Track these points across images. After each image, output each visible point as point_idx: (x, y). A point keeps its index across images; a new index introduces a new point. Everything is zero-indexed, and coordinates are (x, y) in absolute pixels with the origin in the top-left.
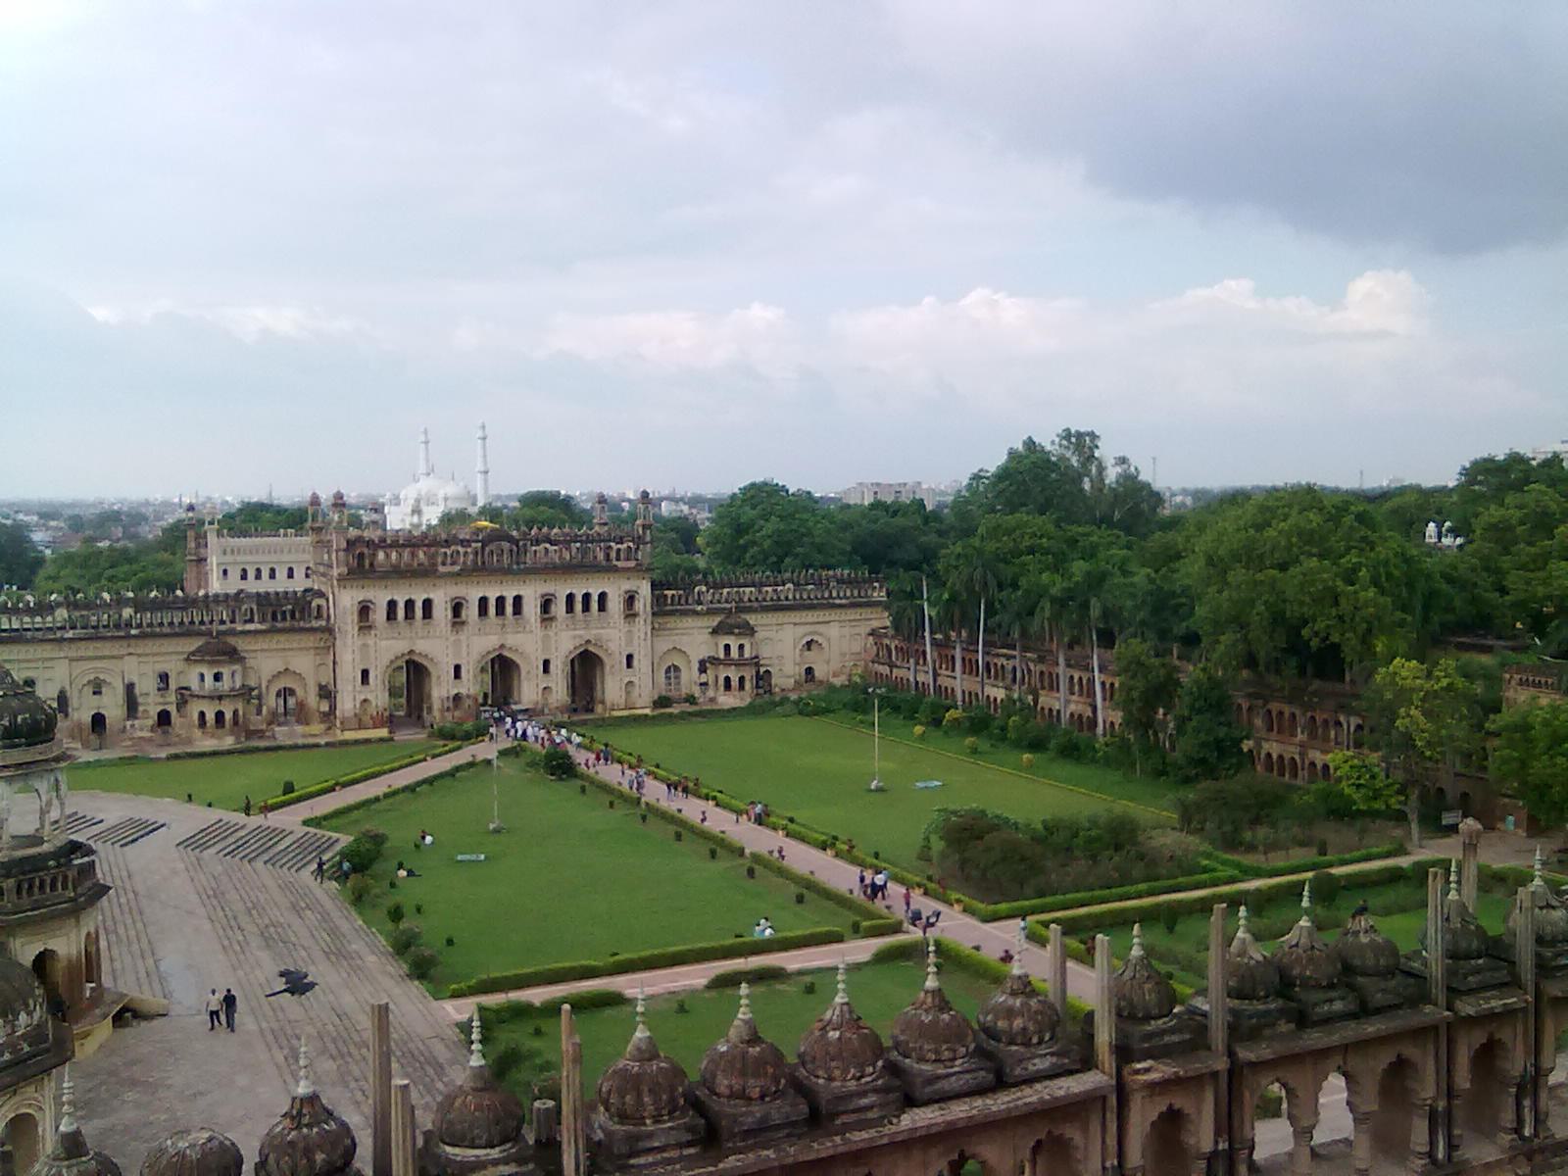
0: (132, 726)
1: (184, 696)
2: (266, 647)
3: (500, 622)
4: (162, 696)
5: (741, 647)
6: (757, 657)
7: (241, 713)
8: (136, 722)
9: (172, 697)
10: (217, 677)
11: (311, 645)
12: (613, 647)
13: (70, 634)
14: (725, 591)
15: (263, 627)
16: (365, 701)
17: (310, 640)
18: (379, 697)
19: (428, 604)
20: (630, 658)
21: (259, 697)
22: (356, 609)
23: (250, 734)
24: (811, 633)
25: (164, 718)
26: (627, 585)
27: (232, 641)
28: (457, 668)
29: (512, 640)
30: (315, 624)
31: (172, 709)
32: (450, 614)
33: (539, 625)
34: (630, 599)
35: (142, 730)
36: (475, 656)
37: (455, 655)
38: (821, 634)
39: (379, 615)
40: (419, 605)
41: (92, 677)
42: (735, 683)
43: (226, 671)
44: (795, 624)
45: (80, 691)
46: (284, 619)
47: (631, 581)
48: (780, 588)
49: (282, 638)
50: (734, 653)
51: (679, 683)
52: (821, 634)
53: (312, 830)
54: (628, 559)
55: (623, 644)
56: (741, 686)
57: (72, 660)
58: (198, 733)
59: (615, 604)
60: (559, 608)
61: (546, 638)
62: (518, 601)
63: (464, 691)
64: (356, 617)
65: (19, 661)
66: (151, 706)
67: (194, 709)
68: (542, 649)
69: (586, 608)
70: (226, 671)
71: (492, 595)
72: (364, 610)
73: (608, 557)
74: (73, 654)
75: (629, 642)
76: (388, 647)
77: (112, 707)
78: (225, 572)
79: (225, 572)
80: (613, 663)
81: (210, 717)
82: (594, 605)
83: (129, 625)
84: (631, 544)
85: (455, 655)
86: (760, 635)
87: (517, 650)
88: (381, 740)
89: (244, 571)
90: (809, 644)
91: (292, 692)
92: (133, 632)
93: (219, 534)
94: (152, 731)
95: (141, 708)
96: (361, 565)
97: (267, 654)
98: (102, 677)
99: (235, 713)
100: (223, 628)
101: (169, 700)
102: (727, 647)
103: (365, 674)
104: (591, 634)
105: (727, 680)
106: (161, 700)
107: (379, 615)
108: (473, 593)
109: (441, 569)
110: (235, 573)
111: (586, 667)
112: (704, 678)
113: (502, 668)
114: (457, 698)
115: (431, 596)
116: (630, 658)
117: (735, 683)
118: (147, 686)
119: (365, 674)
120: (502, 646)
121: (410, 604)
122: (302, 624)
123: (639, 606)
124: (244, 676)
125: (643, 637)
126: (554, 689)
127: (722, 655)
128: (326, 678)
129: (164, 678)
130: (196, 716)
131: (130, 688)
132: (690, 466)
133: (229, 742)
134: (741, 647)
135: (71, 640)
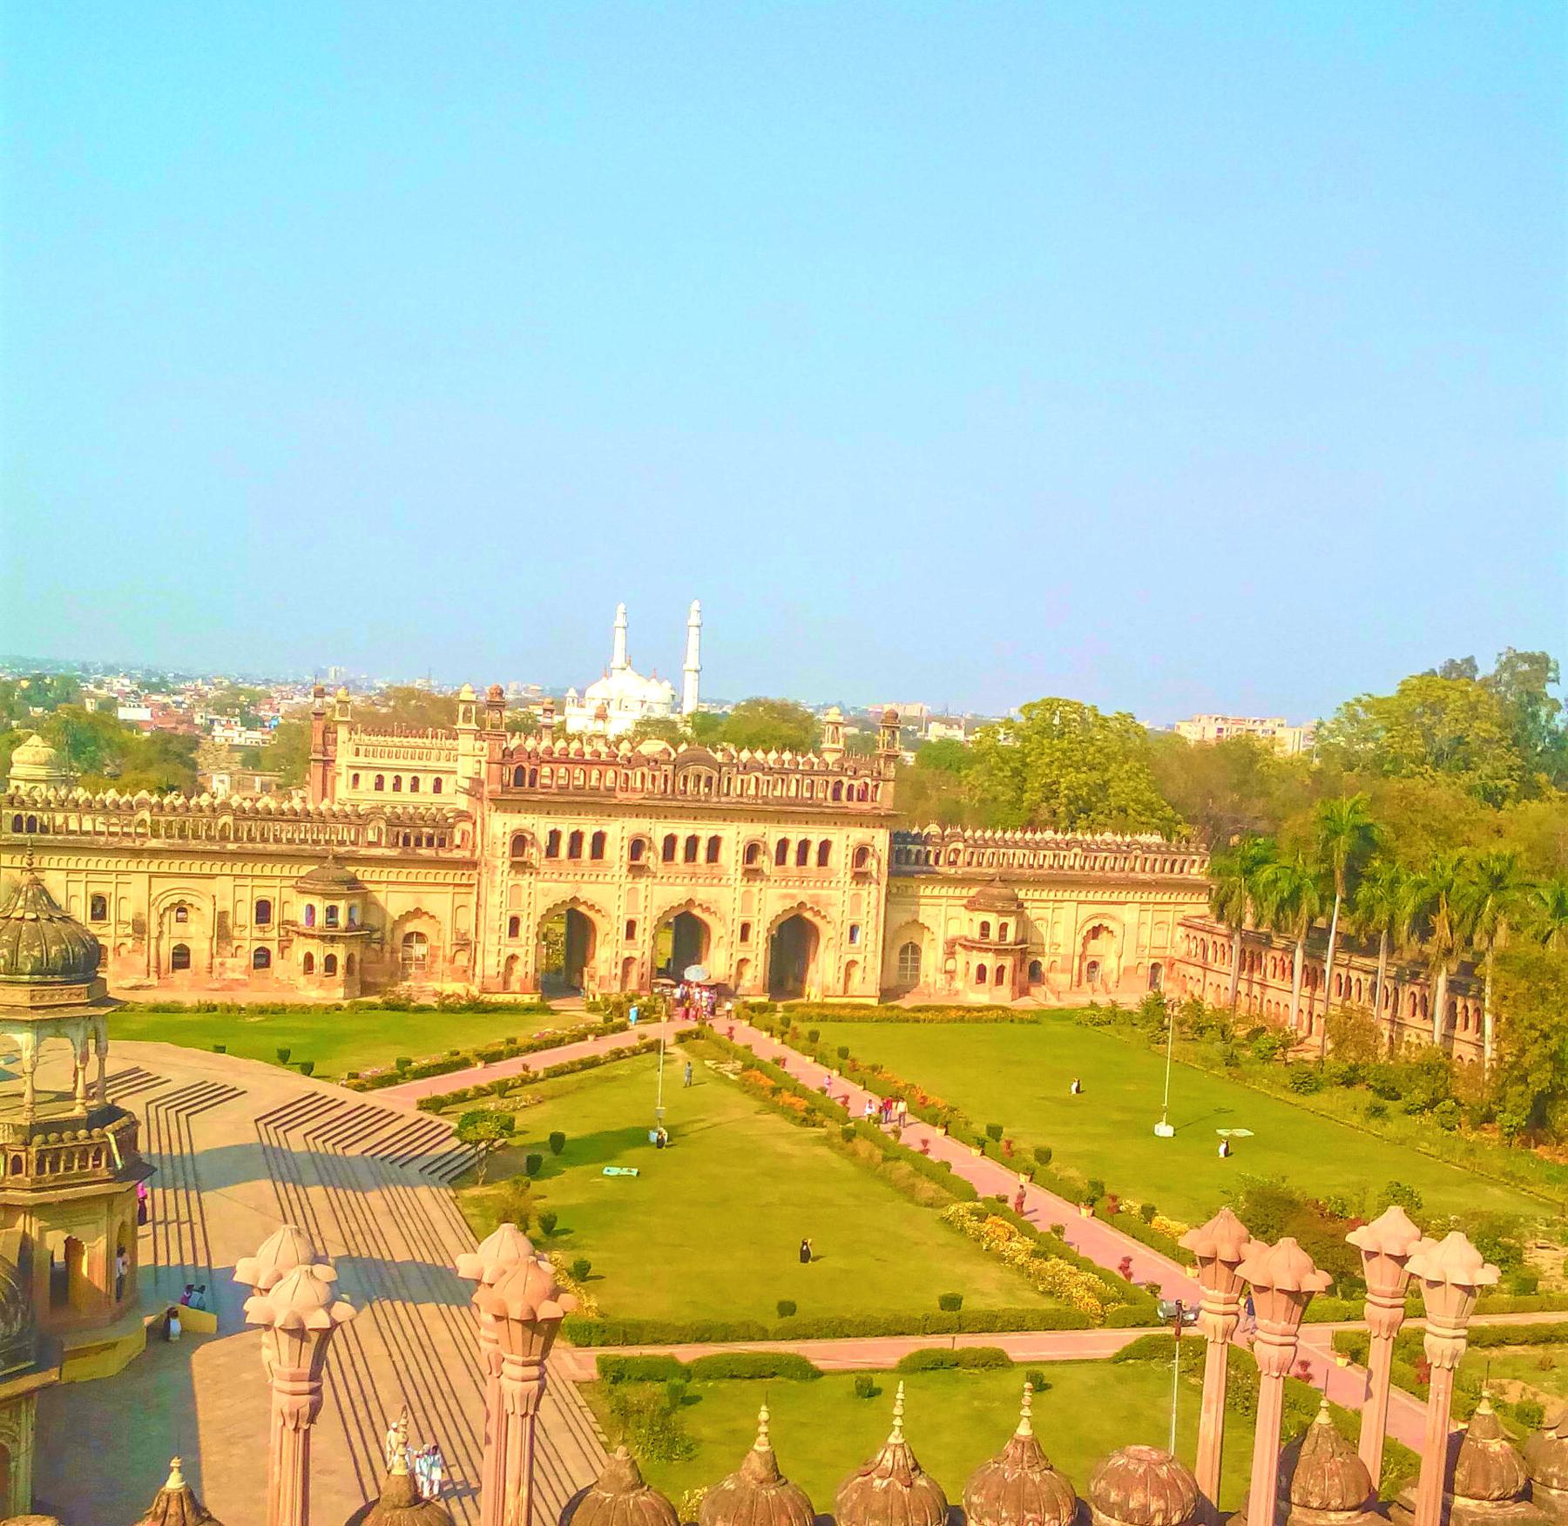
0: (222, 964)
2: (393, 878)
3: (690, 870)
4: (262, 930)
5: (1004, 927)
6: (1023, 941)
7: (357, 958)
8: (230, 962)
9: (275, 934)
10: (332, 911)
11: (449, 880)
12: (834, 913)
13: (153, 843)
14: (989, 851)
15: (394, 853)
16: (513, 958)
17: (450, 876)
18: (527, 949)
19: (599, 839)
20: (853, 930)
21: (381, 941)
22: (508, 839)
23: (367, 988)
24: (1103, 916)
25: (262, 959)
26: (859, 835)
29: (702, 894)
30: (457, 854)
31: (273, 947)
32: (626, 853)
33: (739, 876)
35: (233, 971)
37: (627, 908)
38: (1112, 918)
41: (176, 899)
42: (990, 975)
44: (1080, 902)
45: (161, 916)
46: (418, 843)
47: (864, 830)
48: (1062, 853)
50: (994, 934)
51: (917, 969)
52: (1112, 918)
53: (428, 1116)
54: (862, 799)
55: (847, 908)
56: (999, 981)
57: (152, 875)
58: (302, 980)
59: (840, 858)
63: (636, 954)
64: (507, 849)
65: (89, 872)
66: (249, 938)
67: (300, 948)
68: (742, 909)
69: (802, 859)
71: (683, 830)
72: (520, 842)
73: (836, 797)
74: (153, 868)
75: (856, 907)
76: (545, 891)
78: (356, 777)
79: (356, 777)
80: (830, 933)
81: (319, 960)
82: (813, 857)
83: (225, 838)
84: (868, 780)
85: (627, 908)
86: (1032, 912)
87: (708, 909)
88: (529, 1009)
89: (380, 778)
90: (1096, 932)
91: (421, 937)
92: (231, 847)
93: (352, 730)
94: (244, 973)
95: (236, 943)
96: (519, 782)
97: (396, 888)
98: (189, 899)
99: (350, 959)
100: (342, 850)
101: (267, 935)
102: (985, 926)
103: (515, 923)
104: (803, 895)
105: (982, 970)
106: (256, 934)
108: (658, 830)
109: (621, 796)
110: (368, 779)
111: (793, 940)
112: (950, 965)
113: (688, 932)
114: (628, 961)
115: (604, 829)
116: (853, 930)
117: (990, 975)
119: (515, 923)
120: (690, 902)
122: (443, 854)
123: (871, 864)
124: (365, 911)
125: (873, 903)
126: (754, 962)
127: (976, 934)
128: (466, 922)
129: (263, 911)
130: (301, 959)
131: (223, 915)
132: (965, 681)
133: (338, 995)
134: (1004, 927)
135: (155, 853)
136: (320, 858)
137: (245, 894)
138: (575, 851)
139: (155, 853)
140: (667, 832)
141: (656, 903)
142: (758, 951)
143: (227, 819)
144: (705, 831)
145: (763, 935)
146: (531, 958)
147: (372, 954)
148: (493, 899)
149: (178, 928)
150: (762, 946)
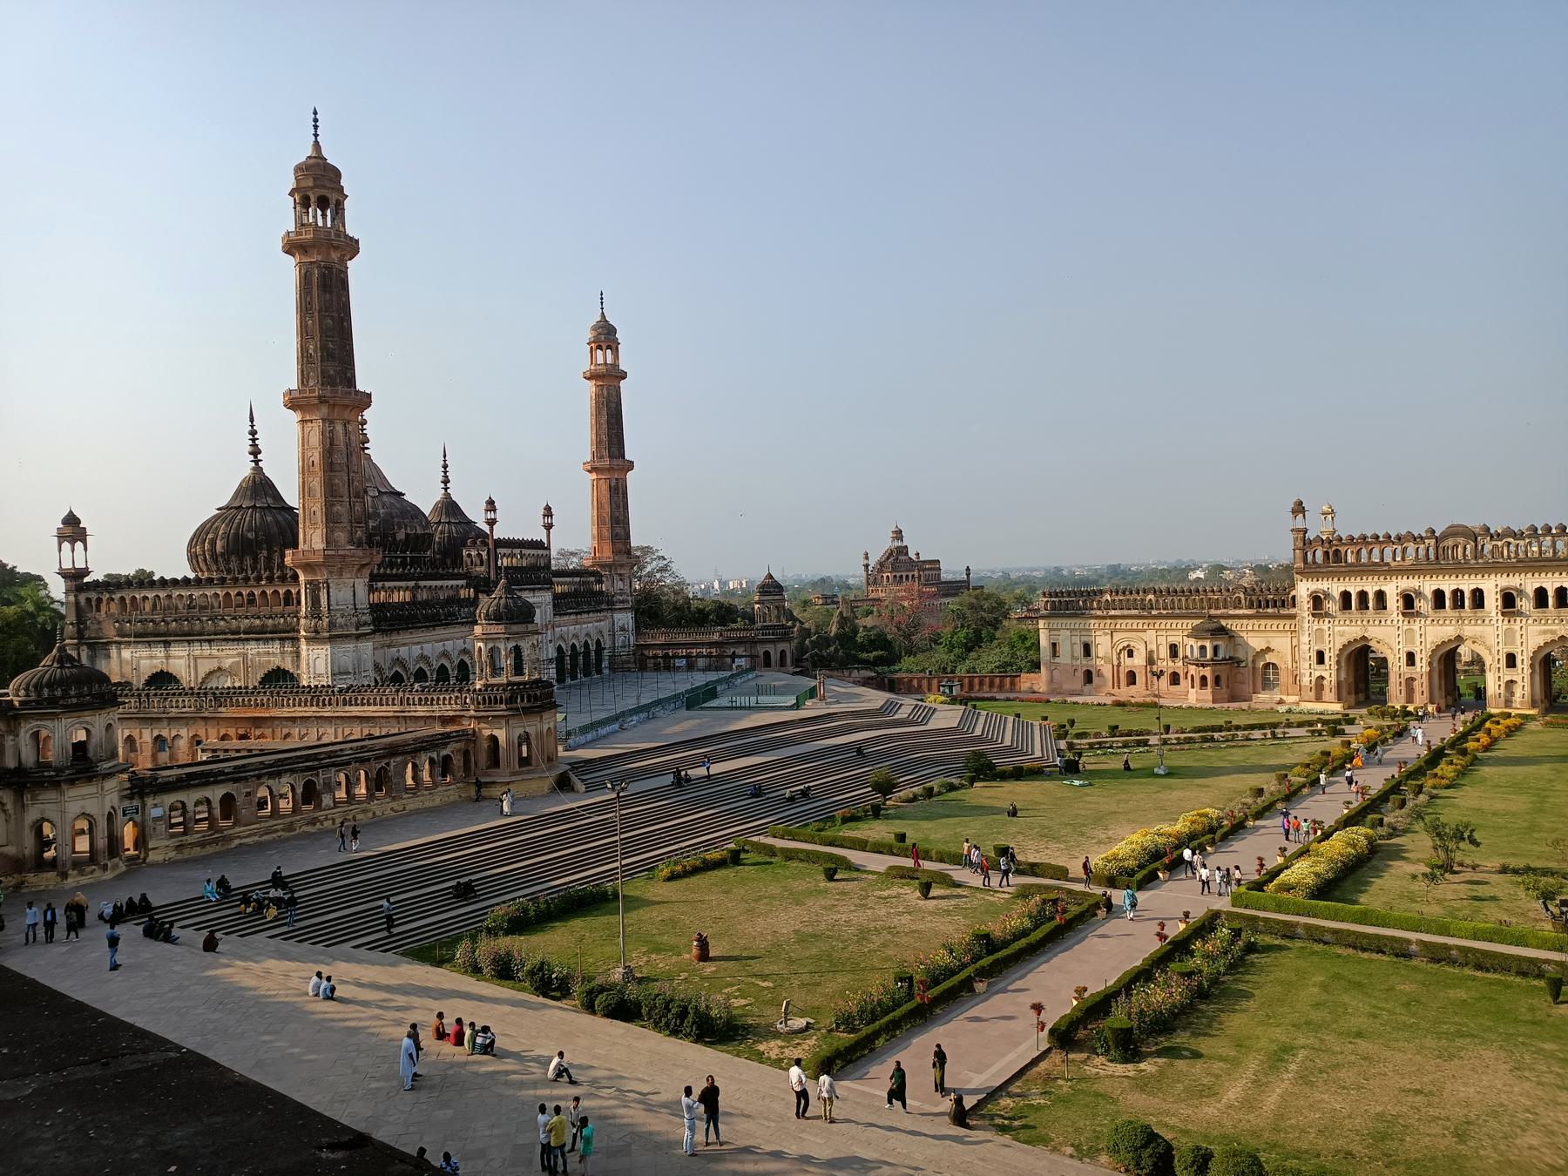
10: (1203, 648)
13: (1112, 612)
19: (1380, 595)
27: (1223, 623)
28: (1411, 658)
29: (1468, 631)
30: (1292, 611)
32: (1401, 603)
36: (1431, 647)
43: (1208, 644)
49: (1263, 622)
61: (1509, 634)
76: (1342, 631)
100: (1219, 612)
118: (1164, 652)
121: (1363, 595)
135: (1112, 617)
137: (1162, 640)
140: (1434, 588)
141: (1429, 640)
142: (1523, 675)
143: (1151, 596)
144: (1467, 584)
145: (1527, 662)
146: (1334, 679)
147: (1233, 672)
148: (1305, 639)
149: (1129, 661)
150: (1527, 671)
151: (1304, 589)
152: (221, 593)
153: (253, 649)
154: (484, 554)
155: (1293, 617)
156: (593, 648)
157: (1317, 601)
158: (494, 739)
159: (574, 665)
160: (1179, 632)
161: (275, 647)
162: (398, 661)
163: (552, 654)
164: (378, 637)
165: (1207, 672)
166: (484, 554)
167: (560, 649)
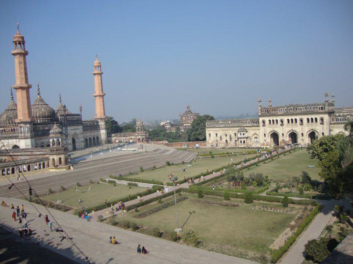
1: (238, 138)
10: (241, 134)
12: (318, 131)
18: (269, 140)
26: (321, 116)
34: (322, 119)
36: (286, 132)
39: (267, 123)
40: (275, 121)
60: (305, 121)
62: (296, 120)
69: (312, 121)
70: (242, 133)
76: (269, 129)
77: (228, 138)
99: (244, 141)
103: (265, 135)
107: (267, 123)
108: (285, 119)
116: (323, 134)
118: (233, 135)
119: (265, 135)
121: (273, 121)
129: (235, 134)
133: (242, 146)
136: (240, 127)
138: (274, 123)
139: (222, 127)
144: (294, 118)
151: (261, 119)
152: (3, 129)
153: (10, 141)
154: (64, 118)
155: (259, 126)
156: (96, 138)
157: (264, 122)
158: (53, 159)
159: (90, 142)
160: (236, 130)
161: (14, 140)
162: (42, 143)
163: (83, 140)
164: (37, 138)
165: (242, 140)
166: (64, 118)
167: (86, 139)
